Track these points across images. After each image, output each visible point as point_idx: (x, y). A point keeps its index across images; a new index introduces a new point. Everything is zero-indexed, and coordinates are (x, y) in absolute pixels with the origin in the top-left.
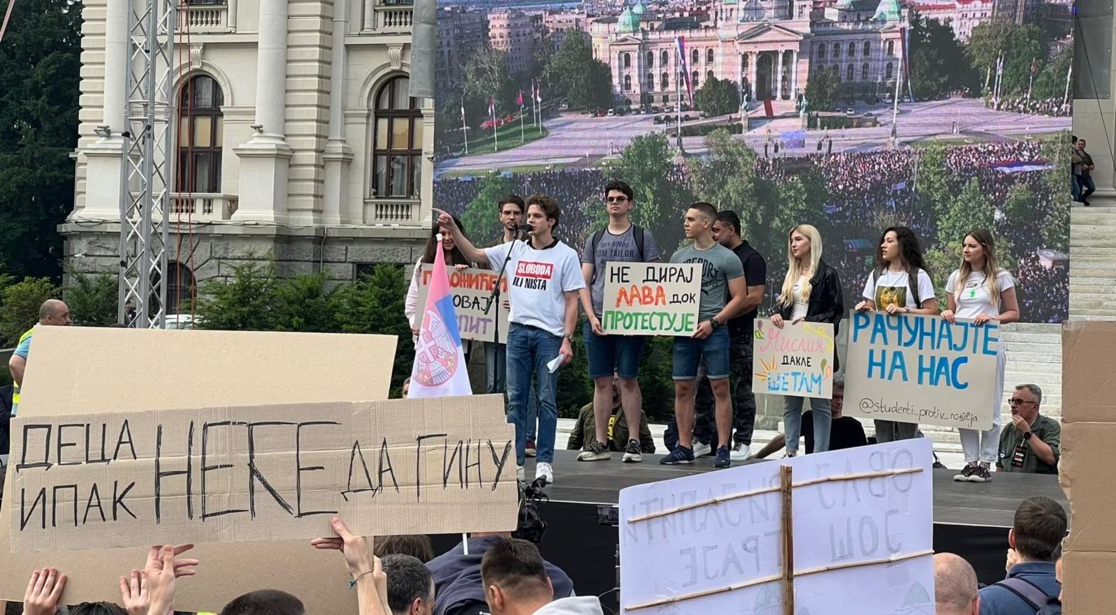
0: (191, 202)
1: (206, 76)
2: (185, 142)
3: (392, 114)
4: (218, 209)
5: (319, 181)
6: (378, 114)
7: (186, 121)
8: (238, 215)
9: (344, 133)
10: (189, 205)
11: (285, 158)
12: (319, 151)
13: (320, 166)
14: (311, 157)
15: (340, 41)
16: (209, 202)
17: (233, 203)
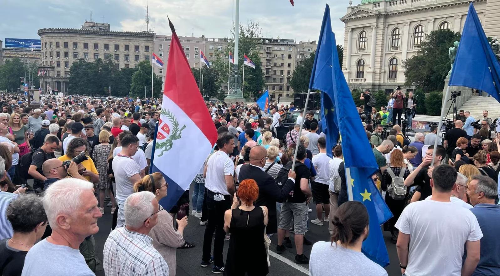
0: (359, 80)
1: (362, 60)
2: (358, 70)
3: (393, 65)
4: (363, 81)
5: (380, 76)
6: (390, 65)
7: (359, 67)
8: (366, 82)
9: (384, 68)
10: (359, 80)
11: (374, 72)
12: (380, 71)
13: (380, 73)
14: (379, 72)
15: (384, 53)
16: (361, 80)
17: (365, 80)
